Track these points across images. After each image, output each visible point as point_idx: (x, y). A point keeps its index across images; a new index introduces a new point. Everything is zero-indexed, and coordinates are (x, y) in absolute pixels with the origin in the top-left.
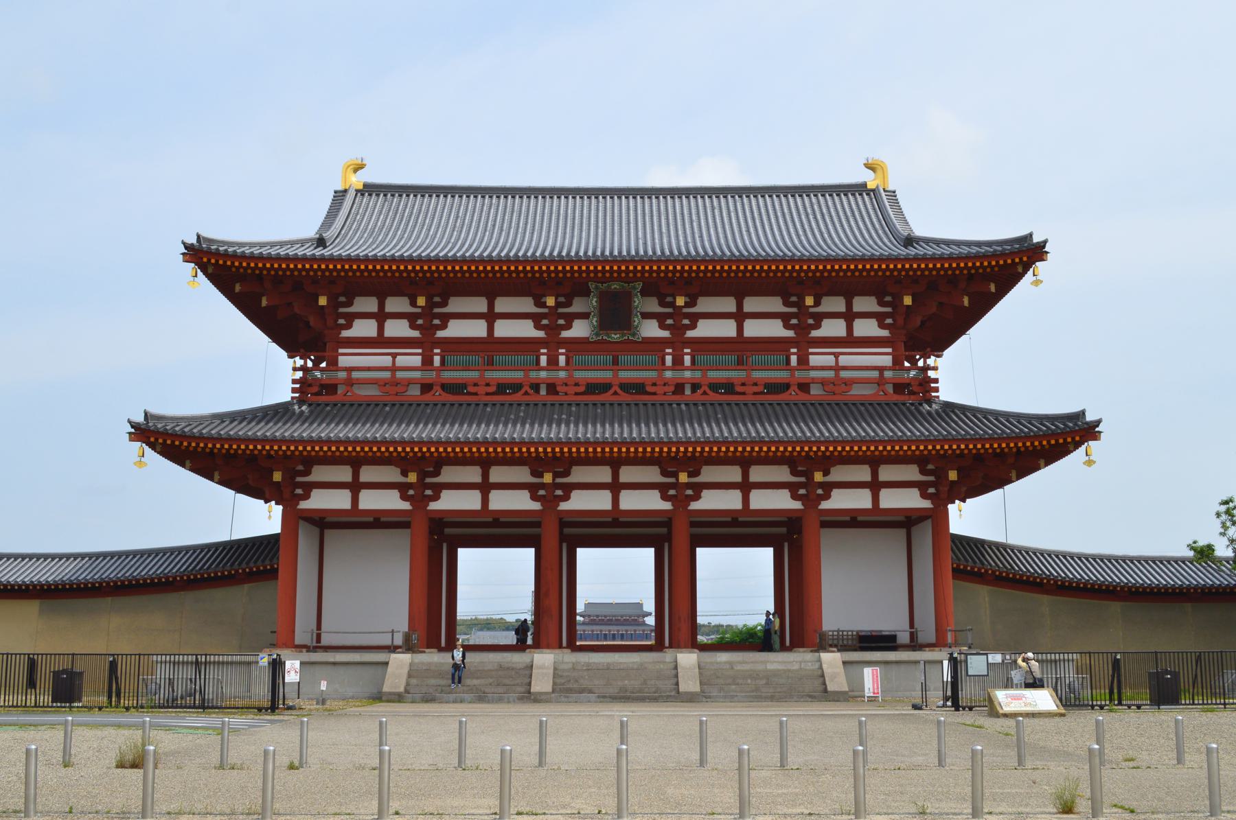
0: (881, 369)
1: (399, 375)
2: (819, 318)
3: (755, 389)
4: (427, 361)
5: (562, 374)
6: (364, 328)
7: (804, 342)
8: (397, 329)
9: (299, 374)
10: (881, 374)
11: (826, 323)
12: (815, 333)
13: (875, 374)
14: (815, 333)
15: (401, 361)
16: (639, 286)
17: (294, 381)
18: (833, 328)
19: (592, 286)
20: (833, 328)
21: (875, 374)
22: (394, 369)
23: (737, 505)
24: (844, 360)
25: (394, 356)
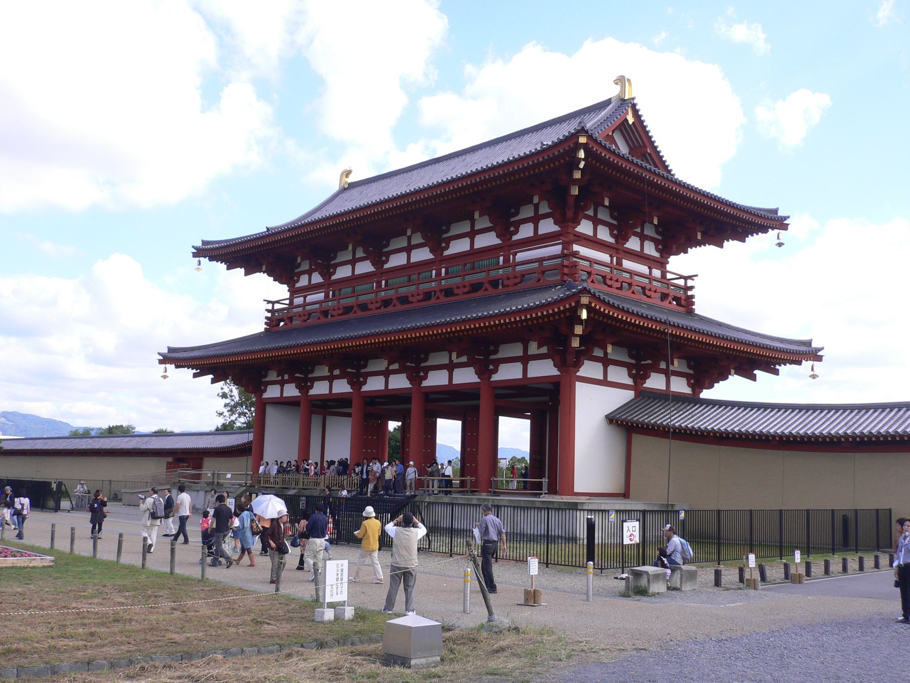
0: (540, 260)
1: (308, 308)
3: (466, 290)
4: (327, 296)
6: (303, 281)
7: (509, 246)
8: (317, 278)
9: (269, 315)
10: (541, 265)
13: (536, 265)
14: (515, 238)
15: (310, 298)
17: (267, 318)
18: (526, 231)
20: (526, 231)
25: (305, 297)
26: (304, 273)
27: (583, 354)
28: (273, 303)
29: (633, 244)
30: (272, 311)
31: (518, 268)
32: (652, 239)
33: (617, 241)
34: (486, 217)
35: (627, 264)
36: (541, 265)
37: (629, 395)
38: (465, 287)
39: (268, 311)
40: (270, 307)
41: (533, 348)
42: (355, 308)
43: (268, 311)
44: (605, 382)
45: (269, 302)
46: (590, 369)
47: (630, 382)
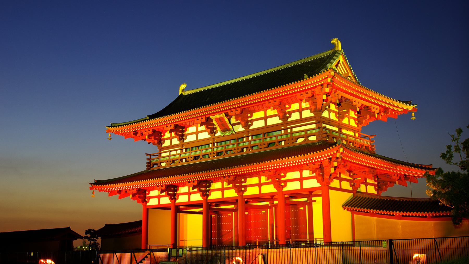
0: (306, 131)
2: (290, 113)
3: (265, 146)
5: (211, 150)
8: (175, 141)
9: (148, 161)
11: (293, 114)
12: (289, 120)
13: (304, 133)
14: (289, 120)
15: (172, 153)
16: (224, 114)
19: (211, 117)
20: (295, 116)
21: (304, 133)
22: (170, 156)
23: (257, 192)
24: (294, 130)
26: (167, 139)
27: (332, 177)
28: (150, 155)
29: (345, 121)
30: (150, 159)
31: (294, 135)
32: (354, 118)
33: (339, 120)
34: (276, 110)
35: (344, 131)
36: (306, 133)
37: (350, 195)
38: (264, 144)
39: (148, 159)
40: (149, 157)
41: (306, 173)
42: (201, 157)
43: (148, 159)
44: (340, 189)
45: (147, 154)
46: (335, 183)
47: (351, 189)
